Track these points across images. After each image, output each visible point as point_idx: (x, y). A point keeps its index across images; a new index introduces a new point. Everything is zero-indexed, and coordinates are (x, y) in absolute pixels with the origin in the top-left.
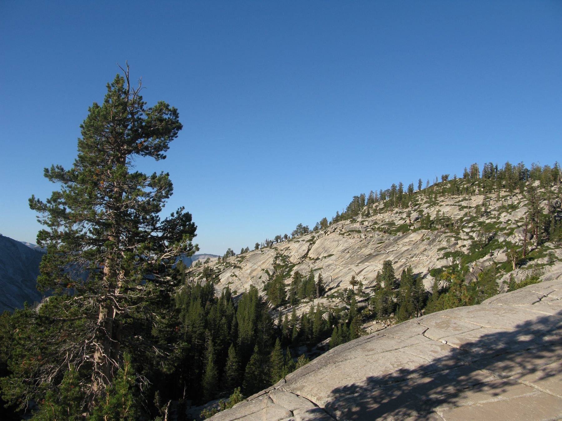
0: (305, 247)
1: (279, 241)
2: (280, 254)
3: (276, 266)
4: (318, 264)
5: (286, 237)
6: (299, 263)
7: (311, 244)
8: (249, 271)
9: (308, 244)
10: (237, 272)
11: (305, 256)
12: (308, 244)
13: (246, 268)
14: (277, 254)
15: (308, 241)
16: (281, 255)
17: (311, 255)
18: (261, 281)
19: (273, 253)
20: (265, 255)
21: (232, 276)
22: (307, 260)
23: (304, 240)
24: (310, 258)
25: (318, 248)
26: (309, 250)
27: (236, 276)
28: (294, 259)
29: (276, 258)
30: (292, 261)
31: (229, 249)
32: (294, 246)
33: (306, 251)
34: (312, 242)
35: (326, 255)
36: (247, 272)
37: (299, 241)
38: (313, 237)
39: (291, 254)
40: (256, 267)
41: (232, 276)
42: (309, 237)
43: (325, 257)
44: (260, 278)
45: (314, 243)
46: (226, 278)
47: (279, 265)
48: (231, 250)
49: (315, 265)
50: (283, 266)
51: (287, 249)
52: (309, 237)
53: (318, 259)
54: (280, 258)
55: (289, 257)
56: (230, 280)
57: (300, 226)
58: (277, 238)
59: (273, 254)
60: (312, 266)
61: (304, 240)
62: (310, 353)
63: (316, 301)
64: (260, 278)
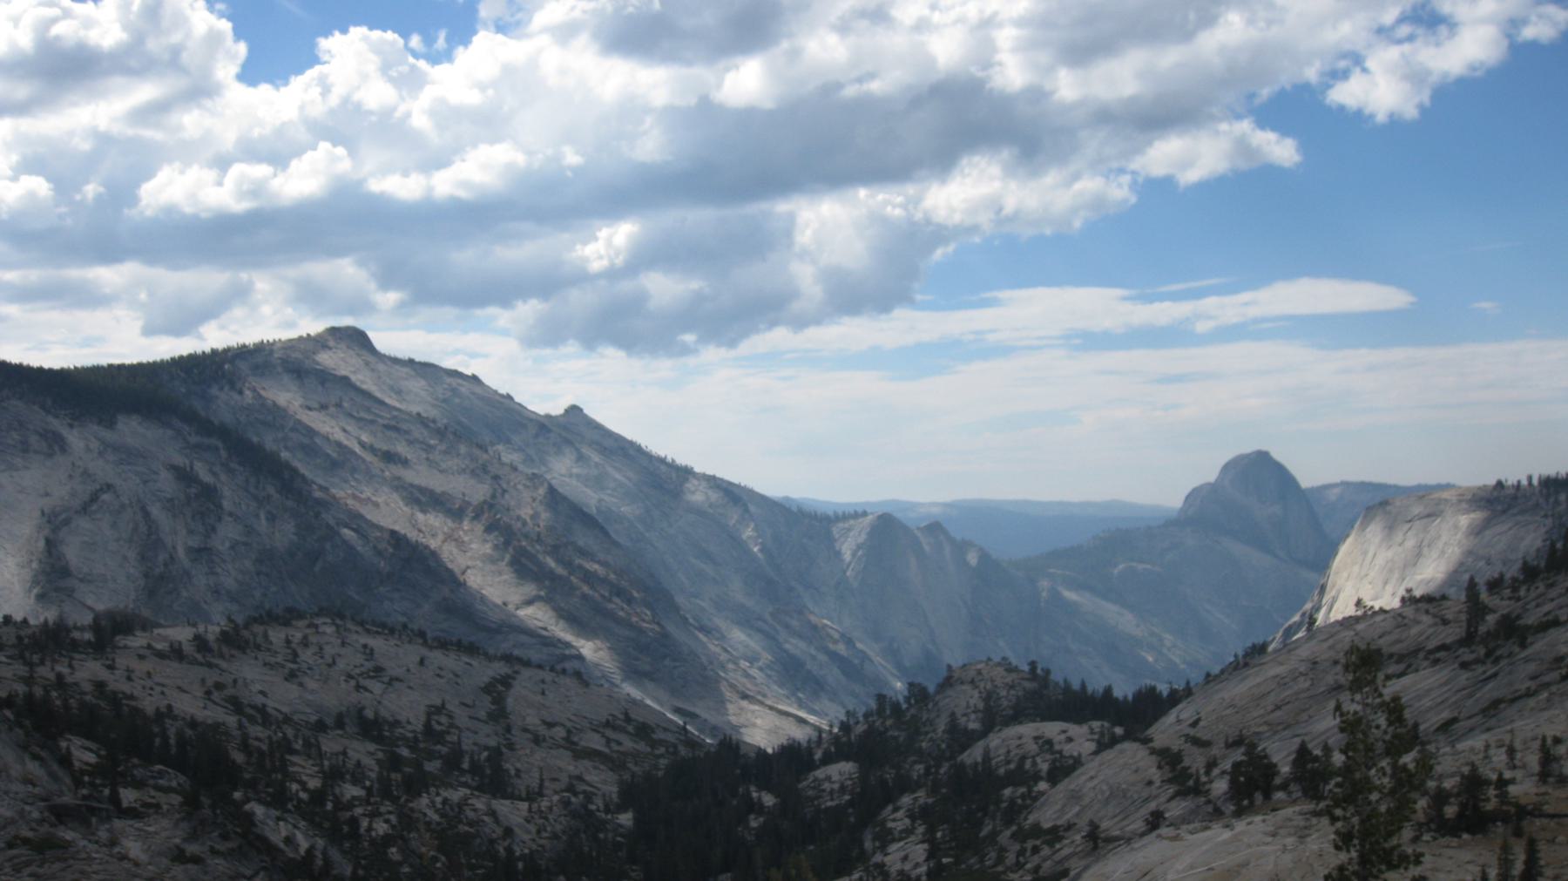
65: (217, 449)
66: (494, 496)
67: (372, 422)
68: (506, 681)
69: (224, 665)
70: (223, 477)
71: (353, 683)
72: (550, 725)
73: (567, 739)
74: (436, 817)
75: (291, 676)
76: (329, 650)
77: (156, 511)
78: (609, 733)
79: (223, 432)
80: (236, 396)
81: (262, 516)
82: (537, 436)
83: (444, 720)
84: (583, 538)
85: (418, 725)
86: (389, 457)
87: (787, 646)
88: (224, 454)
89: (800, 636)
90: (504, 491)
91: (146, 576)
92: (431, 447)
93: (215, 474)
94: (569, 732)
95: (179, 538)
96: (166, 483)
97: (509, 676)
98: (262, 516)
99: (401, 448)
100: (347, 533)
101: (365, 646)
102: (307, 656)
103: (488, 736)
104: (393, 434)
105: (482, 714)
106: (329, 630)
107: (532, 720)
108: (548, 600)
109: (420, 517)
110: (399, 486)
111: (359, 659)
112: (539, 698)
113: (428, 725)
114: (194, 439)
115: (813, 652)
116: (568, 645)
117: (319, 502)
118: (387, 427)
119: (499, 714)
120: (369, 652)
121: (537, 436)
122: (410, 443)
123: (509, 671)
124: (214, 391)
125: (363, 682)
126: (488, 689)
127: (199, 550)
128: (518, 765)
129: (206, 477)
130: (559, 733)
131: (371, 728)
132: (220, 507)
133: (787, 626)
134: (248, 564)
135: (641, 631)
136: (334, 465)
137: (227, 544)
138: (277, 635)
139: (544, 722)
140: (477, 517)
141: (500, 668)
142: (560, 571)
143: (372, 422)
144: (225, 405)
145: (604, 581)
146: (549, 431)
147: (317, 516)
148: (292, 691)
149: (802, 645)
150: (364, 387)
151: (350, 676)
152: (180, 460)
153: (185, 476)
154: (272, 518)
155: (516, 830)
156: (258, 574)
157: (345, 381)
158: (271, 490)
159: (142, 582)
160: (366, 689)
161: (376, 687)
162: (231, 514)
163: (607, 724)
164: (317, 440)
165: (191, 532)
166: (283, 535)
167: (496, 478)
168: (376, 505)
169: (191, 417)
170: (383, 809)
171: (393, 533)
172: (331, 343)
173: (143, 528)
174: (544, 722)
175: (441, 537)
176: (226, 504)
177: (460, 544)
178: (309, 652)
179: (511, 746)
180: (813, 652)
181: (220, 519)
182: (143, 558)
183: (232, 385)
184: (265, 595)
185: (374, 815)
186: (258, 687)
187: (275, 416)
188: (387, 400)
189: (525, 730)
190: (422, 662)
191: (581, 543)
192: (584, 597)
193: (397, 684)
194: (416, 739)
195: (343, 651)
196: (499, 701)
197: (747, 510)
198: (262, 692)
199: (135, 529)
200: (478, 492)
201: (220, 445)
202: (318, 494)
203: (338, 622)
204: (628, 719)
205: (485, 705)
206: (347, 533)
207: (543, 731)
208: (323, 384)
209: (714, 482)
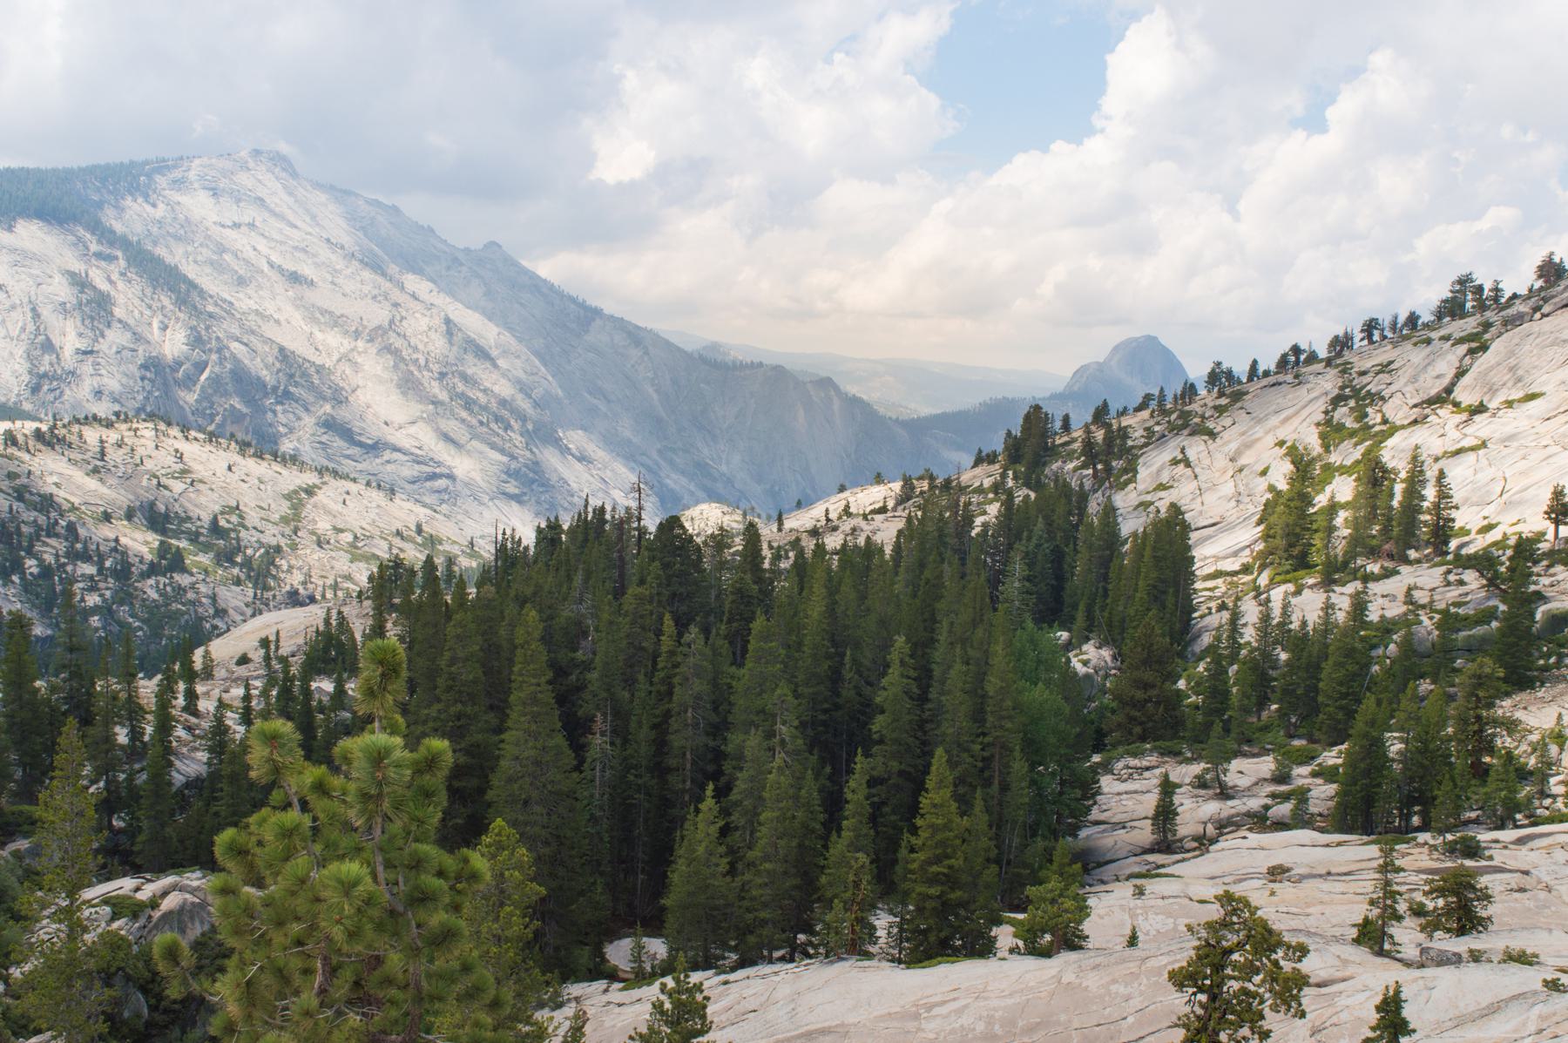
0: (1446, 365)
1: (1376, 337)
2: (1353, 389)
3: (1331, 432)
4: (1482, 427)
5: (1412, 320)
6: (1415, 422)
7: (1471, 352)
8: (1233, 446)
9: (1462, 349)
10: (1196, 448)
11: (1443, 398)
12: (1462, 349)
13: (1226, 435)
14: (1342, 388)
15: (1461, 341)
16: (1356, 393)
17: (1466, 394)
18: (1262, 484)
19: (1329, 383)
20: (1303, 390)
21: (1175, 462)
22: (1445, 412)
23: (1446, 338)
24: (1456, 404)
25: (1492, 368)
26: (1461, 373)
27: (1188, 465)
28: (1398, 408)
29: (1337, 401)
30: (1390, 415)
31: (1219, 364)
32: (1413, 356)
33: (1446, 381)
34: (1478, 344)
35: (1517, 394)
36: (1226, 449)
37: (1428, 342)
38: (1487, 326)
39: (1393, 388)
40: (1259, 431)
41: (1175, 462)
42: (1469, 325)
43: (1509, 404)
44: (1264, 473)
45: (1484, 348)
46: (1154, 468)
47: (1340, 427)
48: (1224, 367)
49: (1469, 430)
50: (1352, 434)
51: (1385, 368)
52: (1469, 325)
53: (1480, 409)
54: (1352, 403)
55: (1383, 399)
56: (1165, 478)
57: (1464, 281)
58: (1370, 327)
59: (1328, 386)
60: (1453, 434)
61: (1446, 338)
62: (1283, 788)
63: (1407, 576)
64: (1264, 473)
65: (116, 258)
66: (392, 322)
67: (281, 243)
68: (310, 491)
69: (26, 457)
70: (121, 285)
71: (155, 481)
72: (339, 531)
73: (353, 545)
74: (155, 596)
75: (96, 471)
76: (140, 451)
77: (46, 312)
78: (397, 541)
79: (124, 243)
80: (149, 208)
81: (156, 324)
82: (448, 268)
83: (234, 519)
84: (474, 368)
85: (206, 519)
86: (295, 278)
87: (668, 481)
88: (122, 263)
89: (683, 473)
90: (402, 318)
91: (30, 372)
92: (340, 272)
93: (111, 282)
94: (356, 537)
95: (69, 338)
96: (62, 290)
97: (315, 486)
98: (156, 324)
99: (307, 270)
100: (235, 346)
101: (177, 451)
102: (114, 456)
103: (272, 536)
104: (301, 255)
105: (276, 517)
106: (150, 434)
107: (324, 525)
108: (430, 420)
109: (319, 335)
110: (299, 303)
111: (170, 460)
112: (340, 507)
113: (215, 521)
114: (94, 247)
115: (692, 487)
116: (439, 464)
117: (211, 316)
118: (296, 248)
119: (293, 520)
120: (180, 457)
121: (448, 268)
122: (317, 265)
123: (317, 481)
124: (129, 201)
125: (164, 481)
126: (288, 497)
127: (85, 353)
128: (293, 562)
129: (103, 286)
130: (348, 537)
131: (157, 519)
132: (112, 314)
133: (671, 463)
134: (133, 369)
135: (513, 457)
136: (241, 282)
137: (114, 349)
138: (92, 435)
139: (335, 528)
140: (371, 340)
141: (310, 478)
142: (443, 396)
143: (281, 243)
144: (133, 217)
145: (485, 408)
146: (461, 264)
147: (208, 328)
148: (92, 483)
149: (684, 481)
150: (277, 210)
151: (156, 477)
152: (78, 266)
153: (80, 282)
154: (164, 328)
155: (231, 612)
156: (143, 379)
157: (260, 201)
158: (166, 302)
159: (26, 378)
160: (166, 487)
161: (178, 486)
162: (120, 321)
163: (398, 533)
164: (227, 257)
165: (80, 335)
166: (174, 344)
167: (396, 305)
168: (277, 322)
169: (97, 228)
170: (102, 585)
171: (282, 349)
172: (251, 164)
173: (31, 327)
174: (335, 528)
175: (336, 357)
176: (118, 312)
177: (356, 366)
178: (121, 452)
179: (294, 547)
180: (692, 487)
181: (109, 326)
182: (29, 357)
183: (146, 197)
184: (146, 398)
185: (93, 589)
186: (55, 479)
187: (186, 231)
188: (299, 224)
189: (313, 533)
190: (230, 468)
191: (469, 372)
192: (463, 421)
193: (200, 486)
194: (198, 534)
195: (154, 453)
196: (297, 507)
197: (646, 353)
198: (56, 484)
199: (23, 329)
200: (379, 315)
201: (120, 254)
202: (210, 308)
203: (162, 426)
204: (419, 530)
205: (284, 508)
206: (235, 346)
207: (331, 535)
208: (238, 201)
209: (620, 324)
